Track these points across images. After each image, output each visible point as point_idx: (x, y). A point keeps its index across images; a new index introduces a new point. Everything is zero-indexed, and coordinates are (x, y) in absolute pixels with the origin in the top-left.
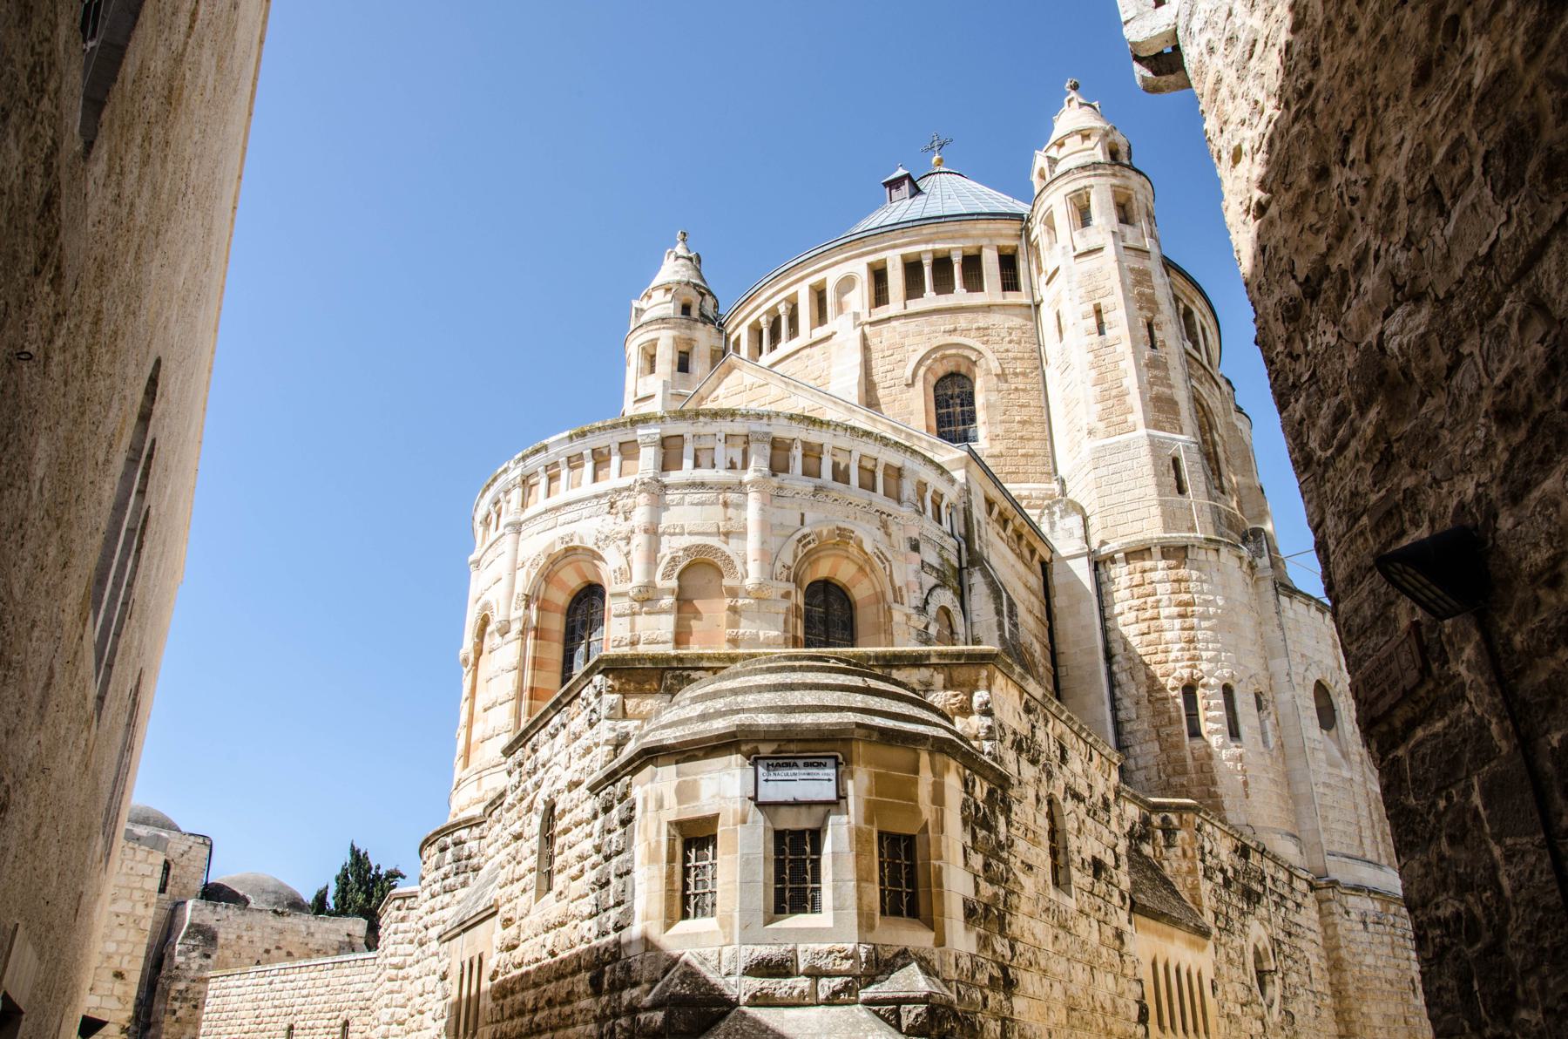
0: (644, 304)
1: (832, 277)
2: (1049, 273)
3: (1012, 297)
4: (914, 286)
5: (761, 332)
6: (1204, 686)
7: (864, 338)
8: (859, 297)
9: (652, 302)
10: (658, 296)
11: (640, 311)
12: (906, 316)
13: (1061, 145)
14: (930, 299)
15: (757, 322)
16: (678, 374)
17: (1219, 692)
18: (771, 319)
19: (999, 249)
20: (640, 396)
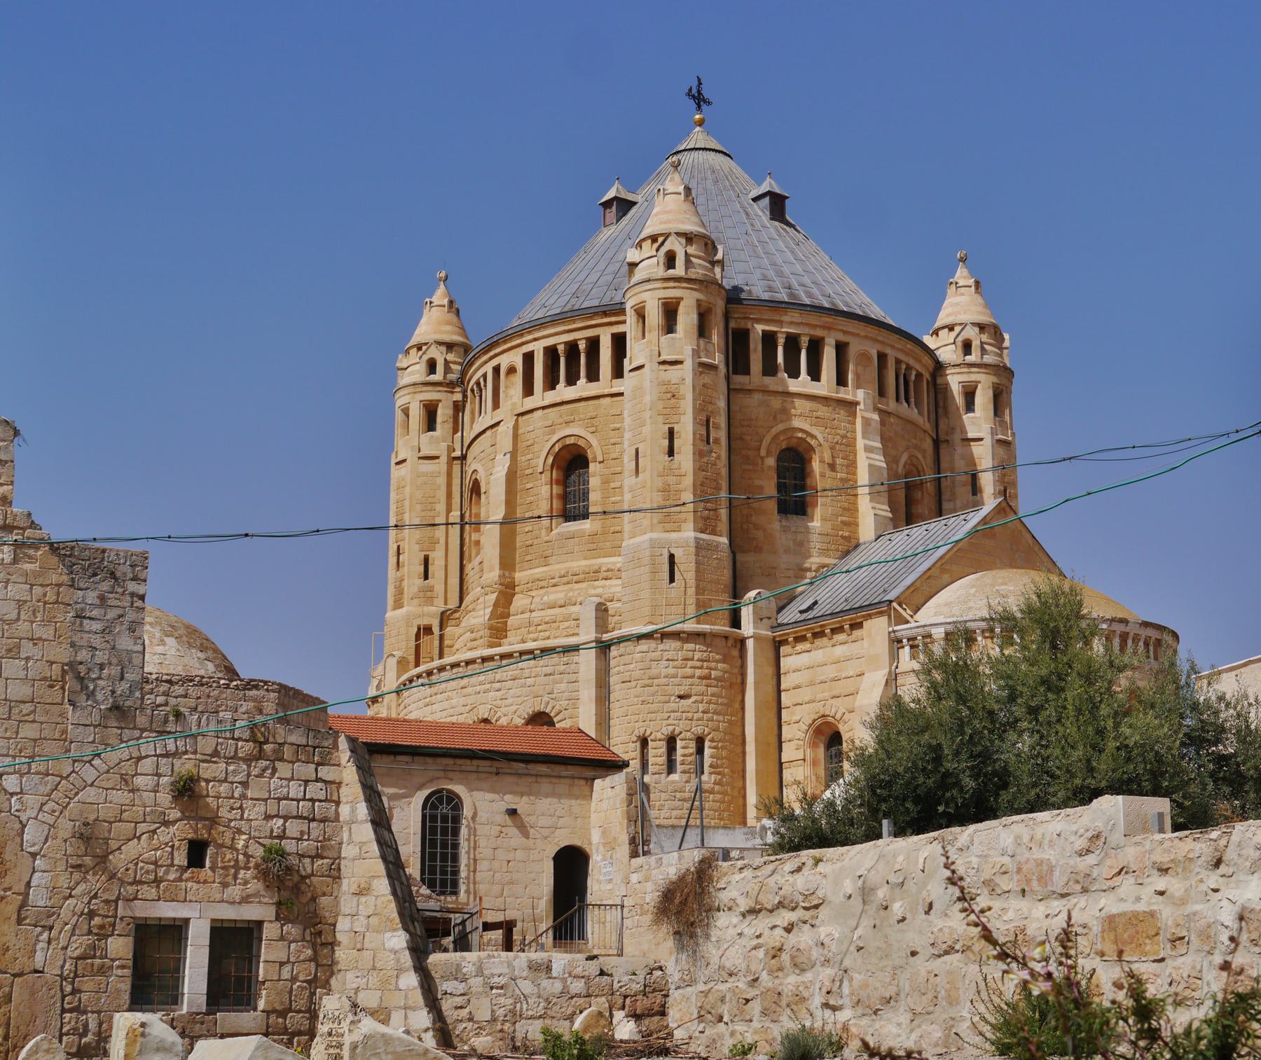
1: (504, 361)
7: (516, 427)
13: (639, 245)
17: (664, 743)
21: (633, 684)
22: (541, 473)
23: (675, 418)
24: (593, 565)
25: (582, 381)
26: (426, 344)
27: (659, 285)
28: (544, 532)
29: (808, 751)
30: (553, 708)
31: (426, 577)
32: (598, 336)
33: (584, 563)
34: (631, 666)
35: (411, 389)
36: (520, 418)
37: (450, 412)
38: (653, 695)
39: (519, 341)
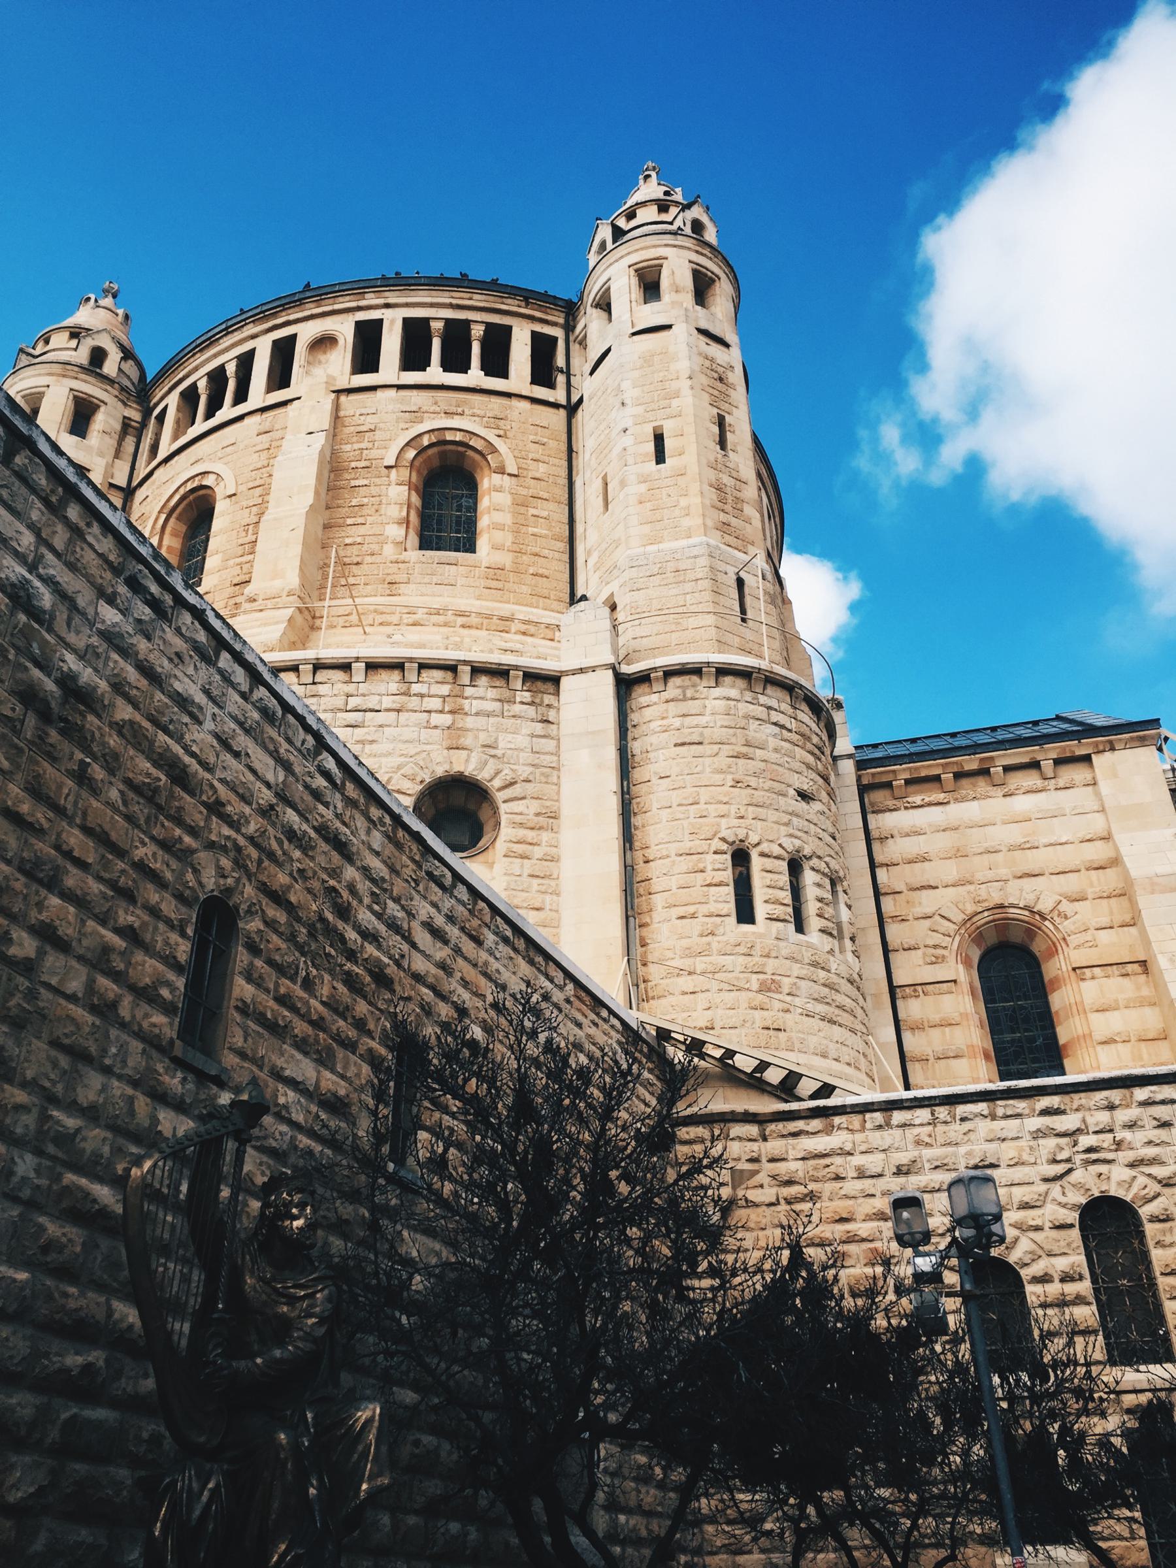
1: (306, 332)
3: (541, 392)
4: (414, 357)
6: (763, 855)
7: (337, 407)
8: (339, 362)
13: (631, 216)
14: (435, 373)
15: (194, 386)
19: (535, 335)
21: (708, 749)
23: (725, 406)
27: (689, 243)
28: (389, 551)
29: (961, 967)
30: (497, 773)
32: (509, 328)
33: (478, 602)
34: (702, 720)
35: (56, 368)
36: (343, 398)
37: (118, 427)
38: (755, 774)
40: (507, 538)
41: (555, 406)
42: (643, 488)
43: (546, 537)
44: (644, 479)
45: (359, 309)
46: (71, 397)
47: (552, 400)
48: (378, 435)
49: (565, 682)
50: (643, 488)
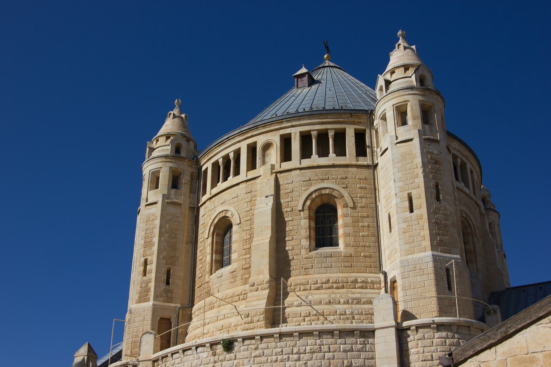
0: (154, 145)
1: (261, 140)
2: (383, 150)
4: (306, 153)
5: (219, 167)
7: (277, 180)
8: (274, 155)
9: (159, 144)
10: (162, 140)
11: (152, 150)
12: (301, 169)
13: (392, 72)
14: (315, 160)
16: (173, 191)
18: (225, 161)
19: (355, 130)
20: (149, 202)
22: (300, 211)
24: (350, 277)
25: (332, 155)
26: (173, 135)
28: (303, 251)
31: (168, 283)
32: (345, 129)
33: (341, 275)
34: (433, 348)
35: (164, 159)
36: (278, 175)
37: (189, 178)
39: (278, 127)
40: (351, 240)
41: (367, 167)
42: (405, 225)
43: (368, 236)
44: (405, 221)
45: (281, 129)
46: (171, 170)
47: (365, 163)
48: (295, 194)
49: (376, 332)
50: (405, 225)
